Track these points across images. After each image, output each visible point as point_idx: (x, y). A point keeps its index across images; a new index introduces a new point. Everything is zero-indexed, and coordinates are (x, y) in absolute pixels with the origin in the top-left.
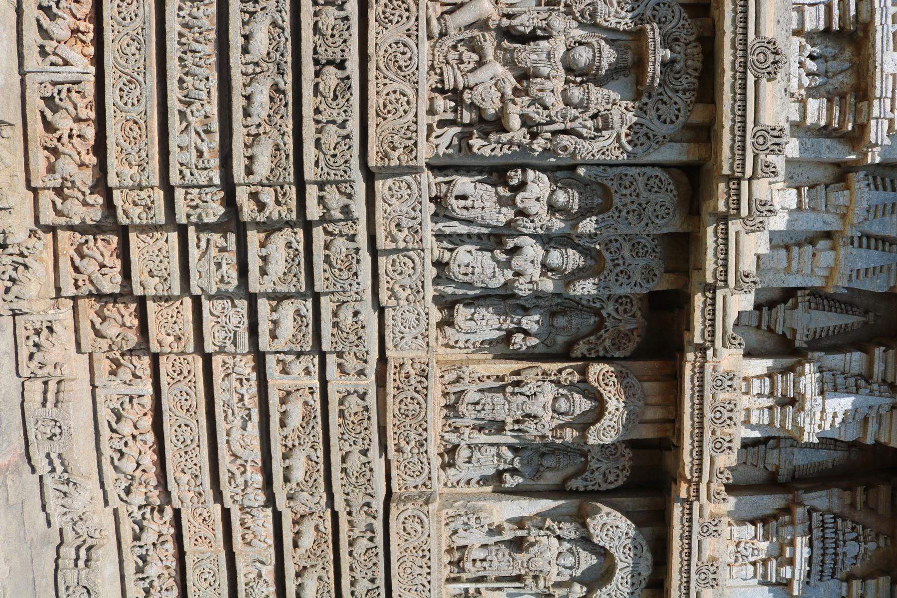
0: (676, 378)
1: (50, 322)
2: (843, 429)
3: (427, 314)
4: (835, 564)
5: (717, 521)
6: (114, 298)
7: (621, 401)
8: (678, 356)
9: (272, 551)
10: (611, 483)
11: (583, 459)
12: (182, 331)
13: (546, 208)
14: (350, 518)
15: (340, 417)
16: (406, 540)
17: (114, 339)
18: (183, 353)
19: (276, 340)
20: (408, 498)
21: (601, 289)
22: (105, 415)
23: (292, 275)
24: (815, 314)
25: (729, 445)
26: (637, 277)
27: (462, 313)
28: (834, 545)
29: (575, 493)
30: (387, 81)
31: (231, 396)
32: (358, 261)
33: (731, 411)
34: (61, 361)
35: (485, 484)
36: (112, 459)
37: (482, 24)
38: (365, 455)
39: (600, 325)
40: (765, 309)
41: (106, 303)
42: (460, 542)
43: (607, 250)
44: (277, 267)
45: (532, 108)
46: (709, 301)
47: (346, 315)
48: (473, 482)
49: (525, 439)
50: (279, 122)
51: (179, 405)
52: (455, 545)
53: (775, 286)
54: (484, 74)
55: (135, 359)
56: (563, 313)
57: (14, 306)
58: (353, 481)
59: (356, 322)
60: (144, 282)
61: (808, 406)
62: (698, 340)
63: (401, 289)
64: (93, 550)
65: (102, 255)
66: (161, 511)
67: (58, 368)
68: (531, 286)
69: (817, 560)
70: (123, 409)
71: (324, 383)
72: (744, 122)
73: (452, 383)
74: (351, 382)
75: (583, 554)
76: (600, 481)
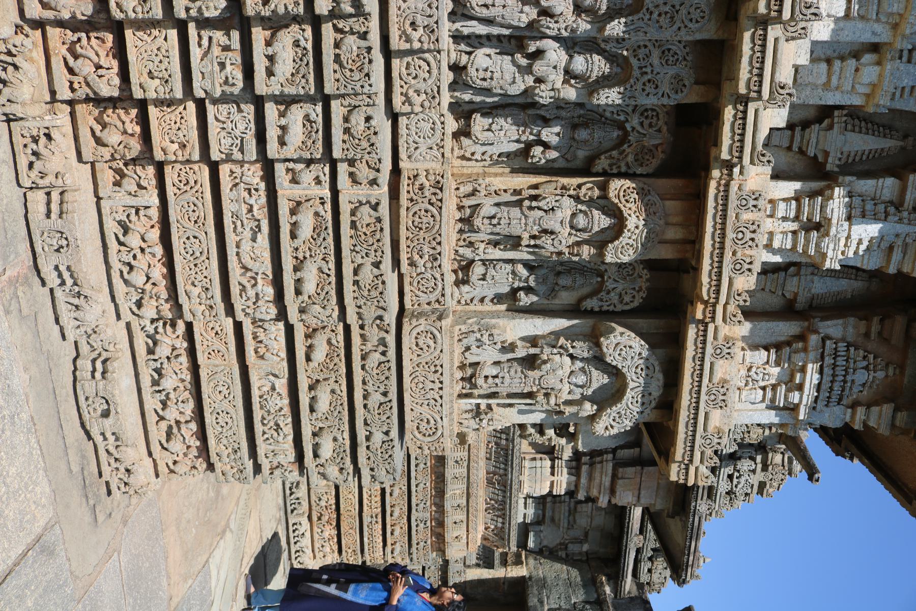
0: (700, 197)
1: (47, 128)
2: (866, 257)
3: (442, 123)
4: (843, 391)
5: (730, 344)
6: (113, 102)
7: (641, 218)
8: (703, 174)
9: (285, 364)
10: (627, 304)
11: (599, 279)
12: (187, 138)
13: (572, 8)
14: (362, 332)
15: (351, 228)
16: (418, 355)
17: (116, 147)
18: (188, 161)
19: (285, 147)
20: (421, 314)
21: (627, 99)
22: (112, 228)
23: (300, 76)
24: (850, 135)
25: (749, 266)
26: (665, 88)
27: (479, 123)
28: (843, 373)
29: (590, 313)
31: (240, 206)
32: (370, 61)
33: (754, 232)
34: (62, 171)
35: (499, 303)
36: (121, 272)
38: (378, 267)
39: (624, 139)
40: (798, 129)
41: (105, 108)
42: (472, 359)
43: (635, 56)
44: (285, 67)
46: (740, 115)
47: (357, 120)
48: (487, 300)
49: (541, 255)
51: (186, 217)
52: (467, 362)
53: (811, 103)
55: (139, 169)
56: (585, 125)
57: (7, 110)
58: (366, 293)
59: (369, 128)
60: (144, 85)
61: (833, 231)
62: (725, 156)
63: (415, 94)
64: (108, 363)
65: (97, 55)
66: (174, 325)
67: (60, 177)
68: (552, 94)
69: (826, 386)
70: (130, 221)
71: (335, 192)
73: (468, 196)
74: (363, 192)
75: (595, 373)
76: (616, 302)
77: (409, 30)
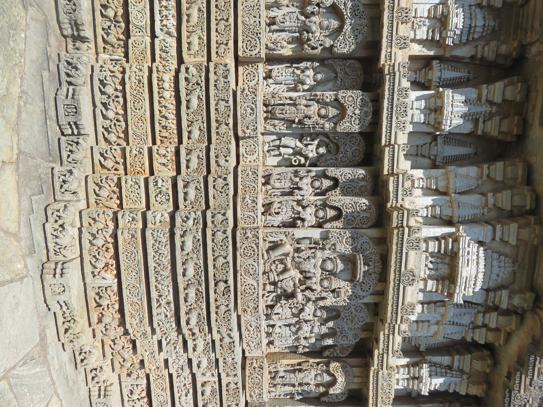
0: (367, 367)
26: (351, 338)
30: (245, 280)
32: (234, 346)
33: (390, 390)
37: (287, 255)
44: (201, 347)
45: (307, 291)
50: (200, 304)
54: (286, 275)
72: (398, 303)
74: (231, 379)
77: (249, 328)
